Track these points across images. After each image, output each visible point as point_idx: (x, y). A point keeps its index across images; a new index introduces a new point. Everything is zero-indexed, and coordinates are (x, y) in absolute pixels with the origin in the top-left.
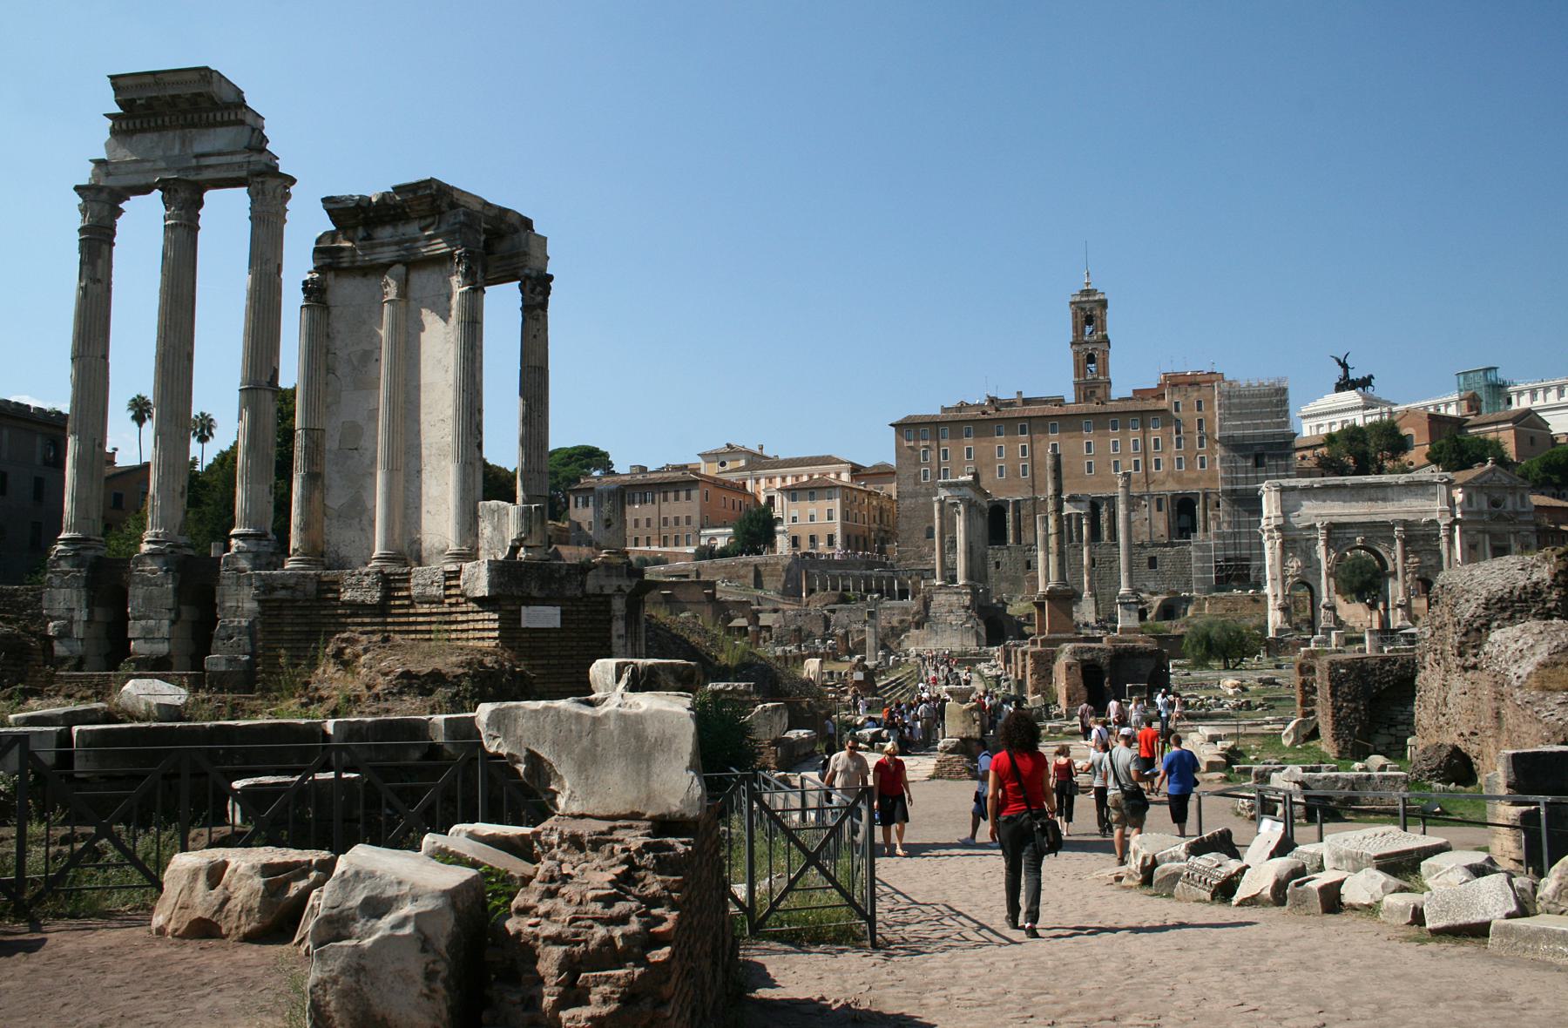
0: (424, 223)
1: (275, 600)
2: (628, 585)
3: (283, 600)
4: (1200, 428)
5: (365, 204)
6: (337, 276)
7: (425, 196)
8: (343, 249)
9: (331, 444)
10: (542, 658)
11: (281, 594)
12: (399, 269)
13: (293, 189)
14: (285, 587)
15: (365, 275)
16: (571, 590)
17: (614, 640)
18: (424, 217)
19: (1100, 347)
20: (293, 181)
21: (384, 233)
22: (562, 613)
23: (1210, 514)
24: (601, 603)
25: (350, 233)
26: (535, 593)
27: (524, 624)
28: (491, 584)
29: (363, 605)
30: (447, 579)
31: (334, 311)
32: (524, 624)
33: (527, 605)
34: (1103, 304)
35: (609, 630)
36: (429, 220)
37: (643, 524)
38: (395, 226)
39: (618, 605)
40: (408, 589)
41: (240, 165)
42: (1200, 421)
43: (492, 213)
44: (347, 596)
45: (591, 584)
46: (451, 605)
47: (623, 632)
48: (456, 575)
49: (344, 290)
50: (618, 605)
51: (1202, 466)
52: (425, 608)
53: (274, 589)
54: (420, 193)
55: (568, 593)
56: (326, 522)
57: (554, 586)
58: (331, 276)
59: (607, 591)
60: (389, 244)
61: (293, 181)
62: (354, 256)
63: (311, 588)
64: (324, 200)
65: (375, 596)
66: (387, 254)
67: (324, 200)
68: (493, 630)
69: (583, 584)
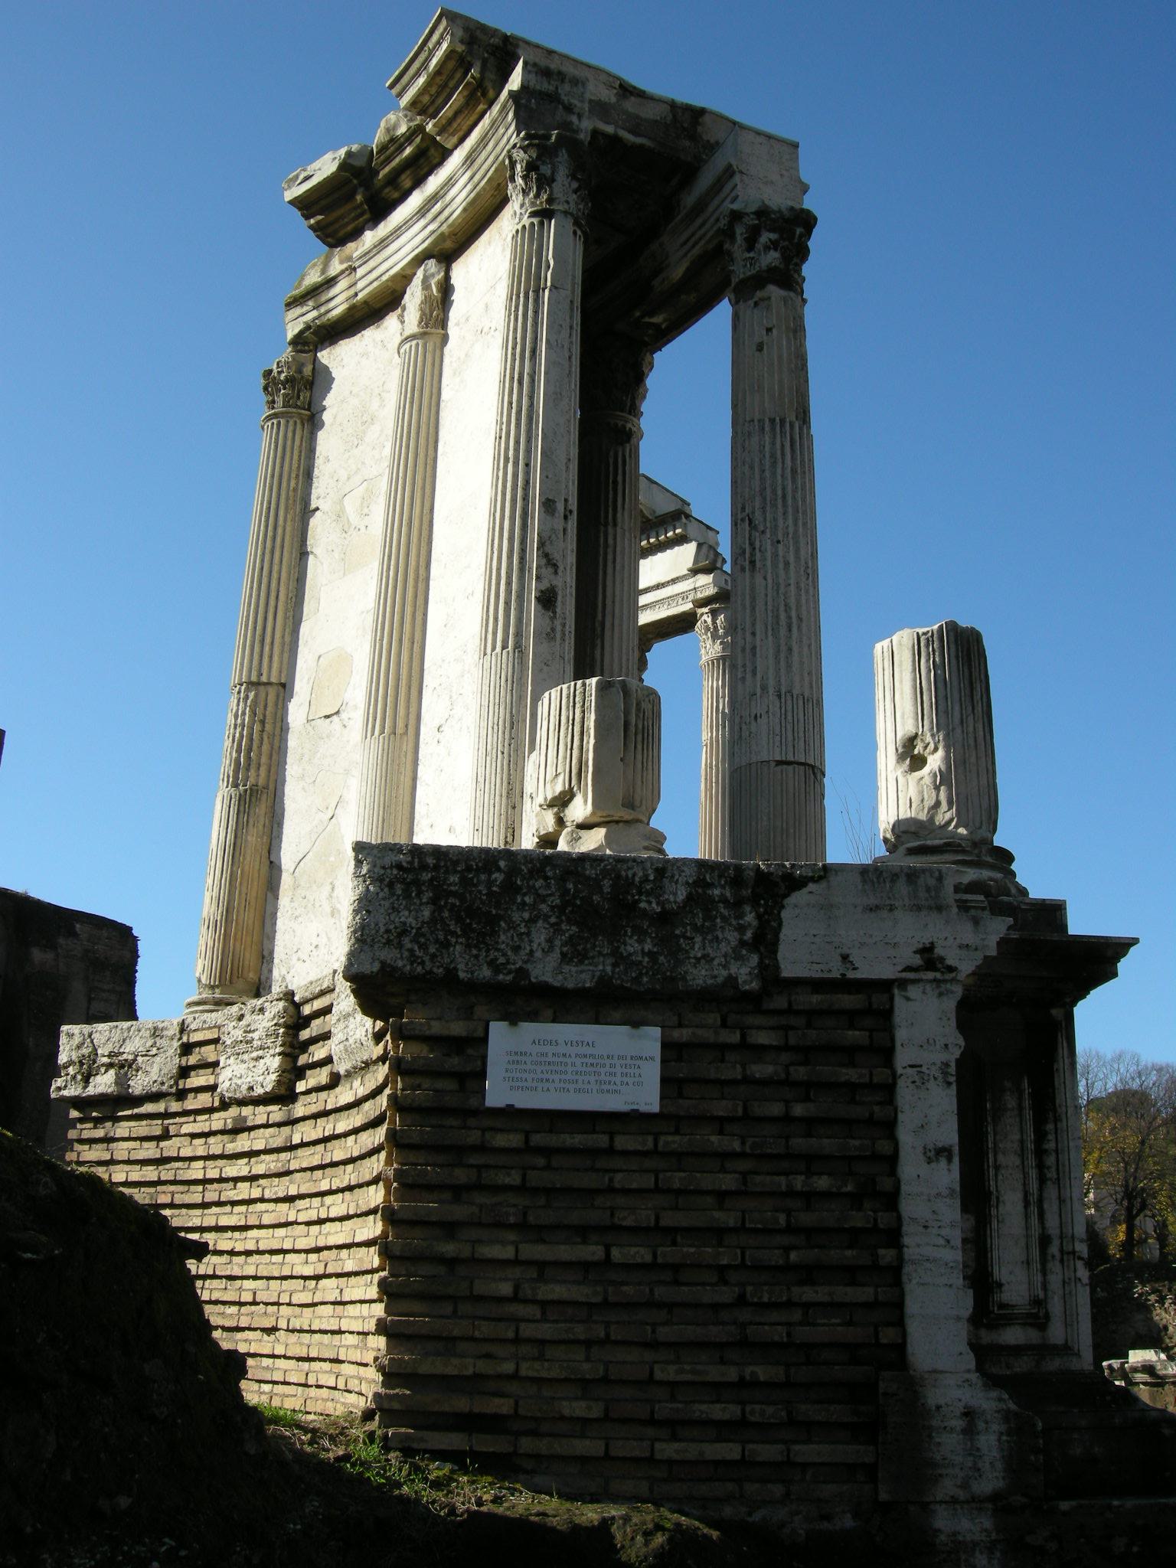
2: (970, 943)
10: (583, 1232)
16: (717, 960)
17: (911, 1166)
24: (851, 1017)
26: (546, 970)
27: (497, 1092)
32: (497, 1092)
33: (513, 1019)
35: (889, 1127)
39: (926, 1032)
41: (683, 595)
43: (650, 112)
45: (804, 948)
47: (949, 1134)
50: (926, 1032)
55: (699, 976)
57: (632, 946)
59: (873, 967)
69: (766, 940)
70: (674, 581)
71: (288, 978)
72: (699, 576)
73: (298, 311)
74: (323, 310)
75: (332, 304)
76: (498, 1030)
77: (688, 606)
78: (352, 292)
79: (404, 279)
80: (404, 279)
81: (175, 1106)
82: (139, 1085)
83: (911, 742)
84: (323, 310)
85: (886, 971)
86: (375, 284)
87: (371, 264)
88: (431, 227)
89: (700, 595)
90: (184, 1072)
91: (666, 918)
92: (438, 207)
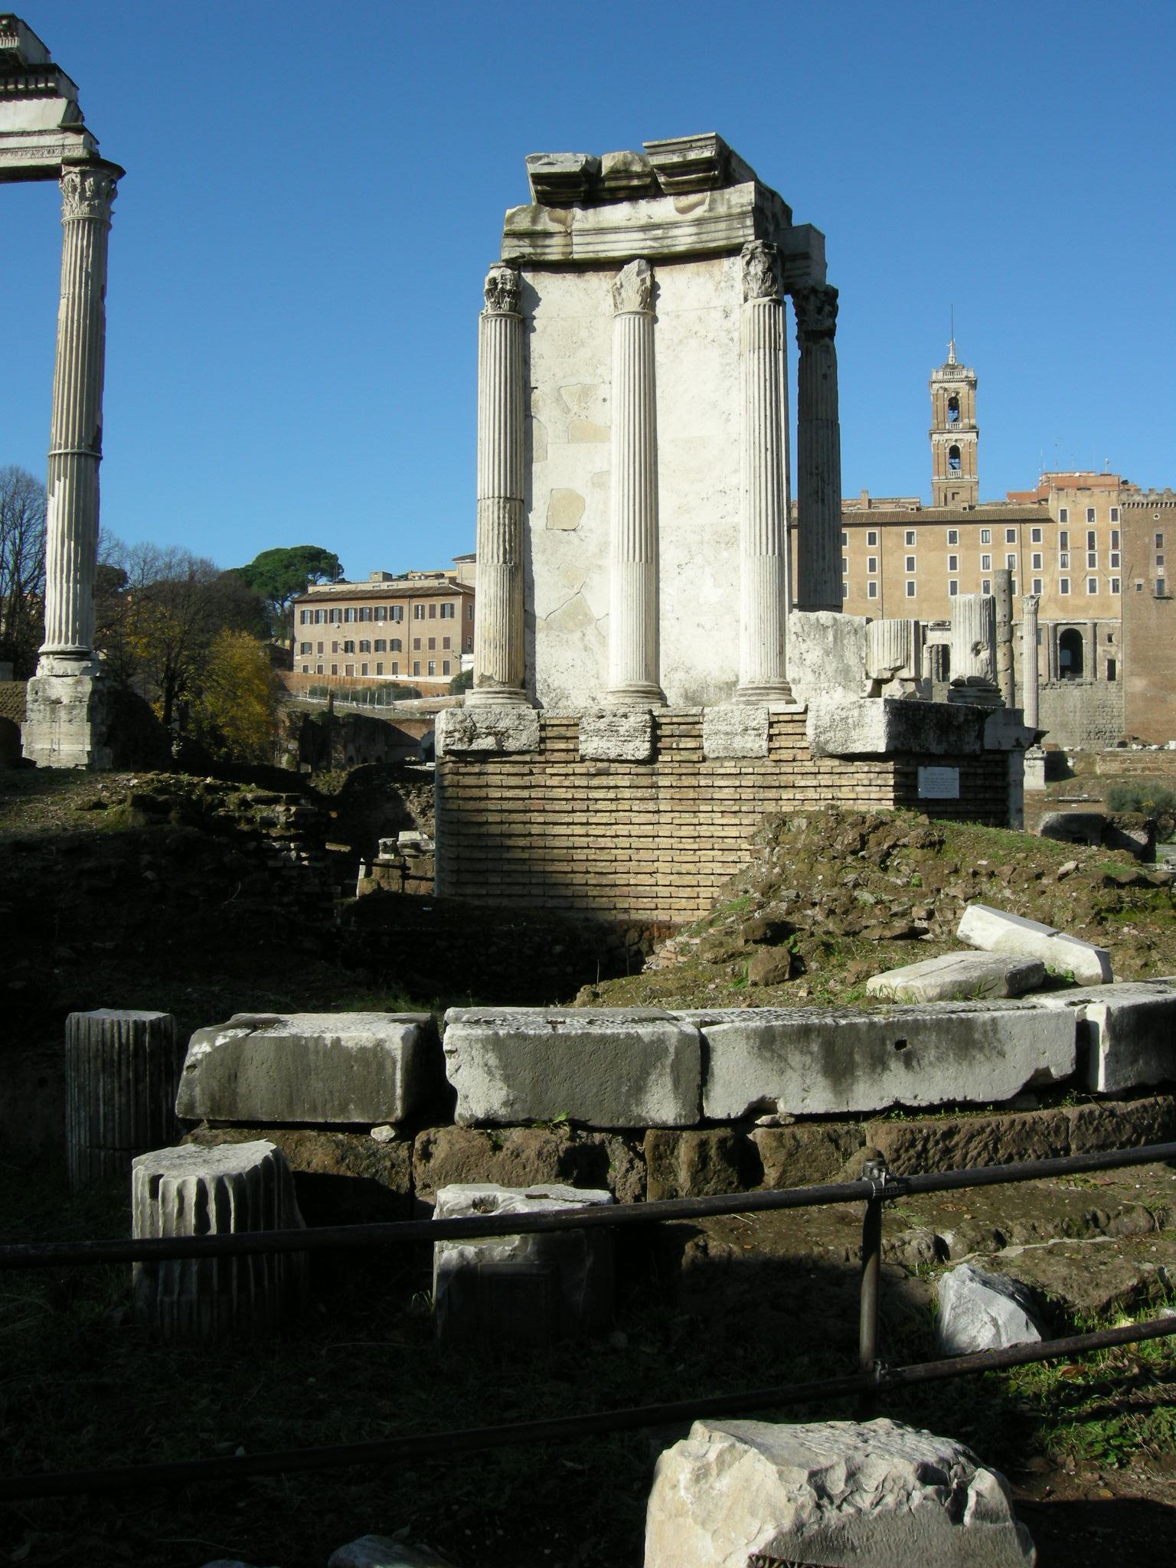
4: (1091, 547)
8: (548, 235)
13: (121, 185)
20: (120, 172)
22: (961, 774)
23: (1099, 649)
26: (935, 749)
28: (892, 736)
30: (771, 725)
37: (439, 643)
41: (50, 149)
42: (1091, 535)
44: (589, 746)
51: (1093, 589)
52: (730, 767)
60: (627, 229)
61: (120, 172)
69: (980, 736)
70: (41, 133)
71: (550, 681)
72: (68, 134)
73: (515, 242)
74: (539, 250)
75: (548, 250)
76: (921, 769)
77: (55, 161)
78: (568, 250)
81: (538, 758)
82: (511, 745)
83: (977, 644)
84: (539, 250)
85: (1009, 747)
86: (591, 255)
87: (588, 239)
88: (650, 243)
89: (67, 154)
90: (542, 740)
91: (959, 728)
92: (659, 232)
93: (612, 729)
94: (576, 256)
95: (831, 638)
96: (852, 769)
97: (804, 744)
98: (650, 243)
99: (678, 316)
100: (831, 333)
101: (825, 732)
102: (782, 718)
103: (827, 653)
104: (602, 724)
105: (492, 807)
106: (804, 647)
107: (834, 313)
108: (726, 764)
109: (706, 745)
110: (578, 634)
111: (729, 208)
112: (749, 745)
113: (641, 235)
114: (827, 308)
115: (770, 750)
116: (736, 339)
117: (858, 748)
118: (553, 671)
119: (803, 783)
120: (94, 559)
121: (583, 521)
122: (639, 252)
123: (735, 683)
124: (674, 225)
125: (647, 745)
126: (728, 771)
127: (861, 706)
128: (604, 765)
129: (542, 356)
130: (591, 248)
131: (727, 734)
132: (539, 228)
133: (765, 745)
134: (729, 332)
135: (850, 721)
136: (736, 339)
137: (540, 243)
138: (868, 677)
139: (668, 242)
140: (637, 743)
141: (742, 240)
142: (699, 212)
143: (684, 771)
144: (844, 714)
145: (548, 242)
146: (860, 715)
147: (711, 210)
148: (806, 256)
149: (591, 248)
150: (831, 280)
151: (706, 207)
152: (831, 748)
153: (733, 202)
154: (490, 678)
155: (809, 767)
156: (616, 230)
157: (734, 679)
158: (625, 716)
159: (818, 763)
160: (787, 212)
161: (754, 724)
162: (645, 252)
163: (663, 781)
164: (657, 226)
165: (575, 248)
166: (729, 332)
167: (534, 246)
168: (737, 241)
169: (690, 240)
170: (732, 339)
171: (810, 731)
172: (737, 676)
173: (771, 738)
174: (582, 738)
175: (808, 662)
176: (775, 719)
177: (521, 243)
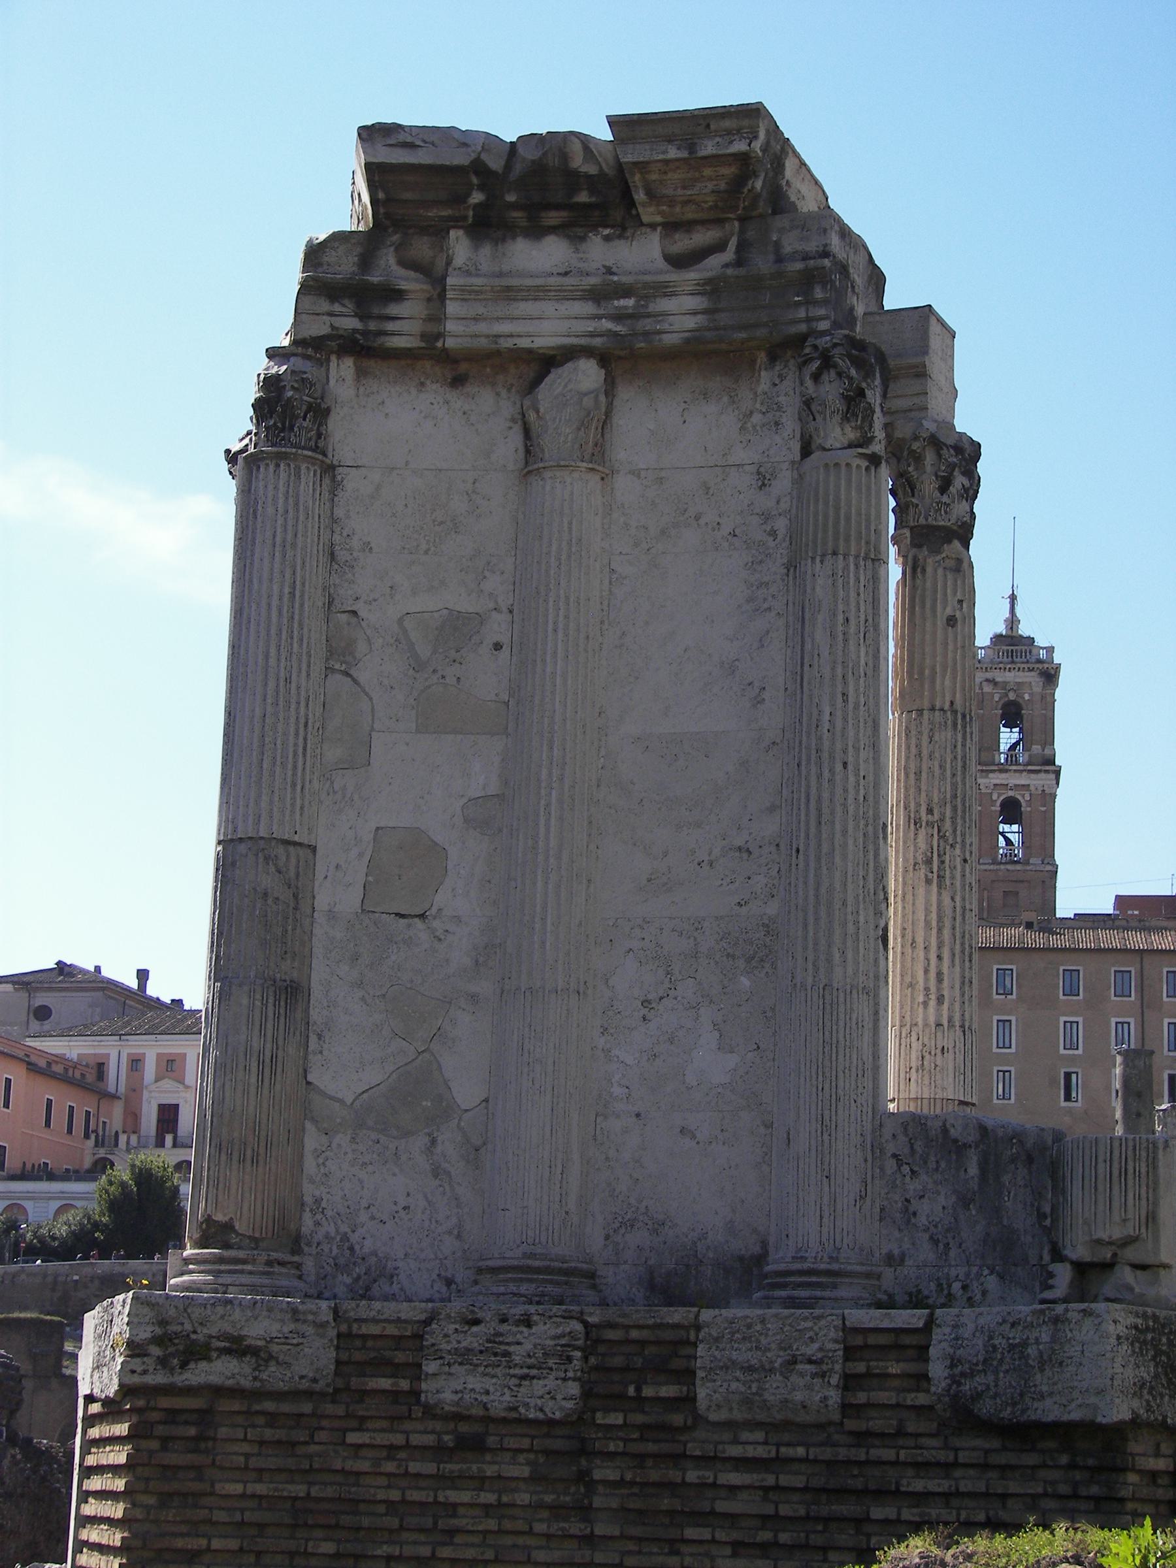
0: (683, 243)
1: (189, 1391)
3: (217, 1391)
5: (495, 164)
6: (361, 374)
7: (715, 160)
9: (336, 892)
11: (220, 1370)
12: (587, 375)
14: (237, 1347)
15: (458, 381)
18: (687, 226)
19: (1037, 781)
21: (540, 256)
25: (422, 248)
29: (514, 1421)
30: (850, 1353)
31: (352, 482)
34: (1050, 676)
36: (702, 237)
38: (577, 240)
40: (687, 1375)
44: (448, 1386)
46: (862, 1437)
48: (914, 1345)
49: (387, 426)
52: (754, 1446)
53: (195, 1352)
54: (708, 148)
56: (312, 1140)
58: (342, 370)
60: (564, 295)
62: (437, 317)
63: (315, 1358)
64: (369, 134)
65: (555, 1395)
66: (548, 325)
67: (369, 134)
68: (115, 1469)
71: (354, 1238)
74: (373, 326)
75: (390, 326)
79: (547, 362)
80: (547, 362)
84: (373, 326)
88: (607, 325)
93: (496, 1352)
94: (450, 343)
95: (973, 1171)
96: (1031, 1459)
97: (922, 1399)
98: (607, 325)
99: (660, 481)
100: (964, 532)
101: (972, 1374)
102: (872, 1340)
103: (965, 1201)
104: (473, 1339)
105: (220, 1516)
106: (913, 1186)
107: (971, 492)
108: (745, 1436)
109: (702, 1393)
110: (421, 1141)
111: (779, 260)
112: (798, 1396)
113: (588, 308)
114: (960, 481)
115: (845, 1407)
116: (781, 533)
117: (1049, 1411)
118: (363, 1217)
119: (919, 1485)
120: (961, 618)
121: (440, 899)
122: (583, 341)
123: (760, 1259)
124: (664, 290)
125: (574, 1389)
126: (751, 1452)
127: (1056, 1320)
128: (472, 1435)
129: (367, 547)
130: (482, 328)
131: (750, 1369)
132: (375, 279)
133: (834, 1397)
134: (766, 517)
135: (1032, 1351)
136: (781, 533)
137: (376, 311)
138: (1057, 1255)
139: (647, 324)
140: (551, 1382)
141: (803, 328)
142: (714, 264)
143: (651, 1447)
144: (1017, 1336)
145: (393, 309)
146: (1054, 1339)
147: (739, 262)
148: (921, 373)
149: (482, 328)
150: (967, 420)
151: (729, 255)
152: (985, 1408)
153: (787, 249)
154: (228, 1227)
155: (933, 1450)
156: (538, 293)
157: (757, 1250)
158: (528, 1323)
159: (956, 1442)
160: (877, 280)
161: (811, 1350)
162: (597, 342)
163: (604, 1472)
164: (626, 291)
165: (450, 326)
166: (766, 517)
167: (362, 318)
168: (794, 330)
169: (691, 323)
170: (773, 533)
171: (937, 1370)
172: (764, 1244)
173: (850, 1382)
174: (431, 1367)
175: (922, 1220)
176: (859, 1341)
177: (337, 308)
